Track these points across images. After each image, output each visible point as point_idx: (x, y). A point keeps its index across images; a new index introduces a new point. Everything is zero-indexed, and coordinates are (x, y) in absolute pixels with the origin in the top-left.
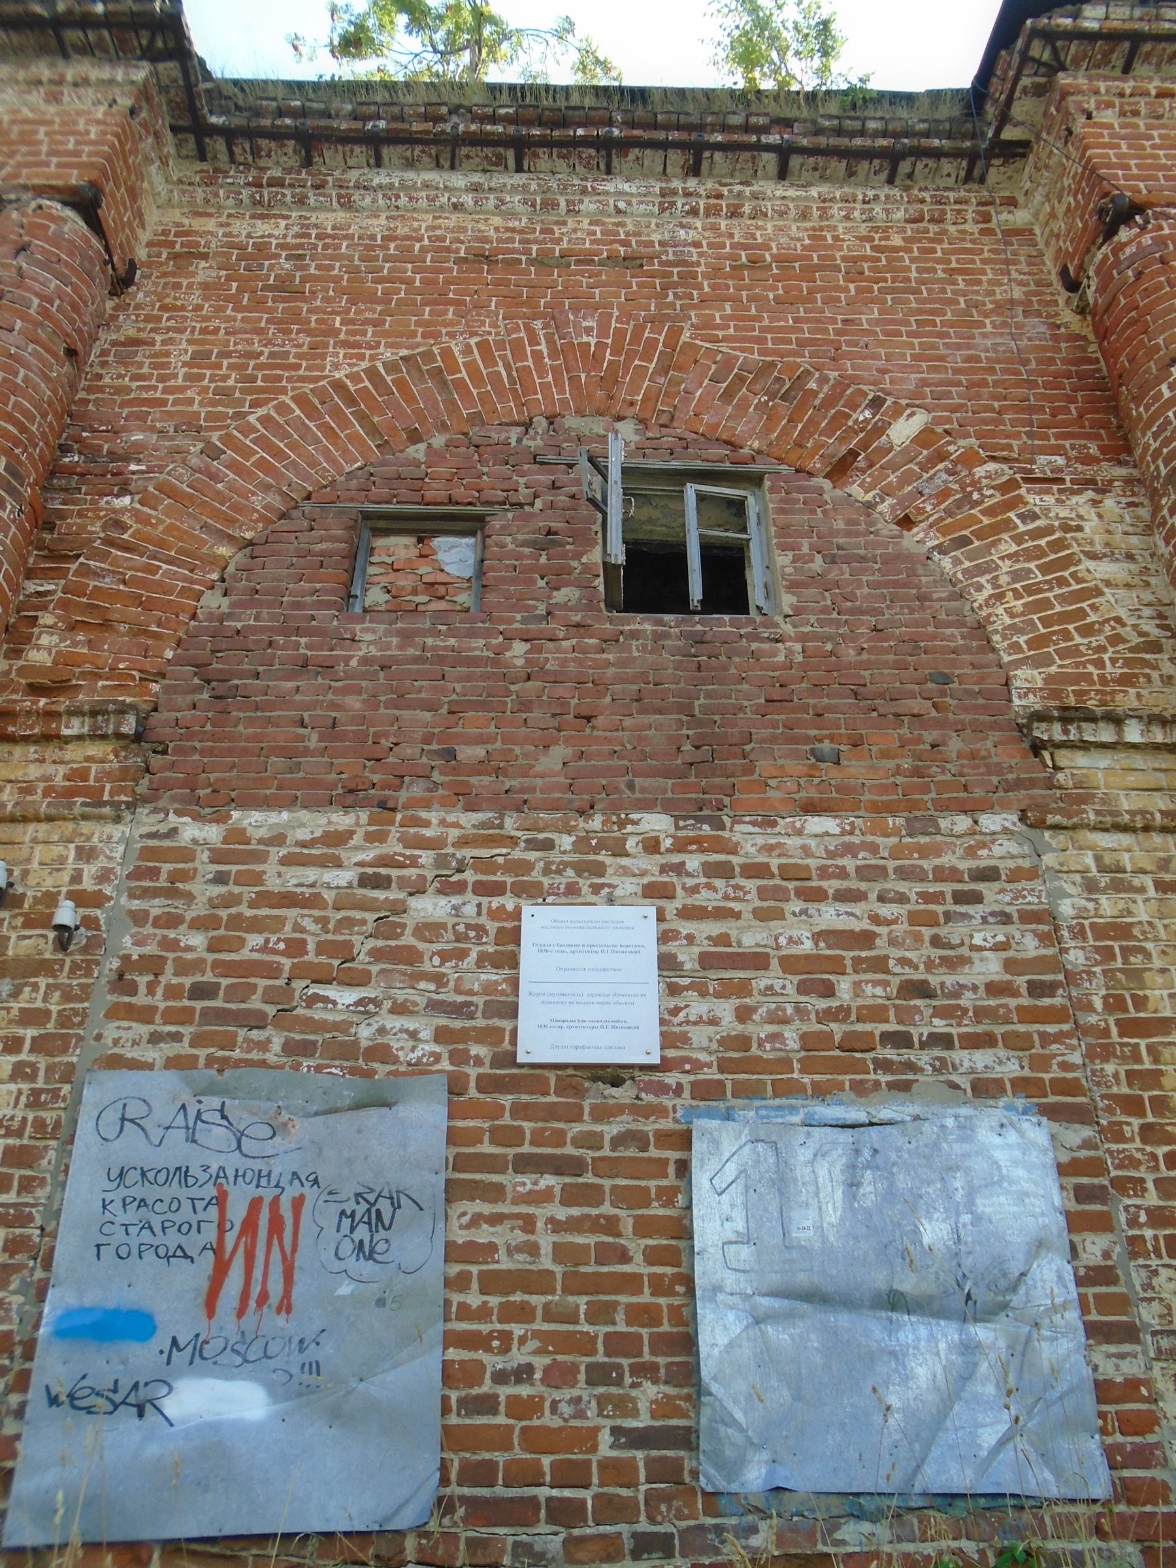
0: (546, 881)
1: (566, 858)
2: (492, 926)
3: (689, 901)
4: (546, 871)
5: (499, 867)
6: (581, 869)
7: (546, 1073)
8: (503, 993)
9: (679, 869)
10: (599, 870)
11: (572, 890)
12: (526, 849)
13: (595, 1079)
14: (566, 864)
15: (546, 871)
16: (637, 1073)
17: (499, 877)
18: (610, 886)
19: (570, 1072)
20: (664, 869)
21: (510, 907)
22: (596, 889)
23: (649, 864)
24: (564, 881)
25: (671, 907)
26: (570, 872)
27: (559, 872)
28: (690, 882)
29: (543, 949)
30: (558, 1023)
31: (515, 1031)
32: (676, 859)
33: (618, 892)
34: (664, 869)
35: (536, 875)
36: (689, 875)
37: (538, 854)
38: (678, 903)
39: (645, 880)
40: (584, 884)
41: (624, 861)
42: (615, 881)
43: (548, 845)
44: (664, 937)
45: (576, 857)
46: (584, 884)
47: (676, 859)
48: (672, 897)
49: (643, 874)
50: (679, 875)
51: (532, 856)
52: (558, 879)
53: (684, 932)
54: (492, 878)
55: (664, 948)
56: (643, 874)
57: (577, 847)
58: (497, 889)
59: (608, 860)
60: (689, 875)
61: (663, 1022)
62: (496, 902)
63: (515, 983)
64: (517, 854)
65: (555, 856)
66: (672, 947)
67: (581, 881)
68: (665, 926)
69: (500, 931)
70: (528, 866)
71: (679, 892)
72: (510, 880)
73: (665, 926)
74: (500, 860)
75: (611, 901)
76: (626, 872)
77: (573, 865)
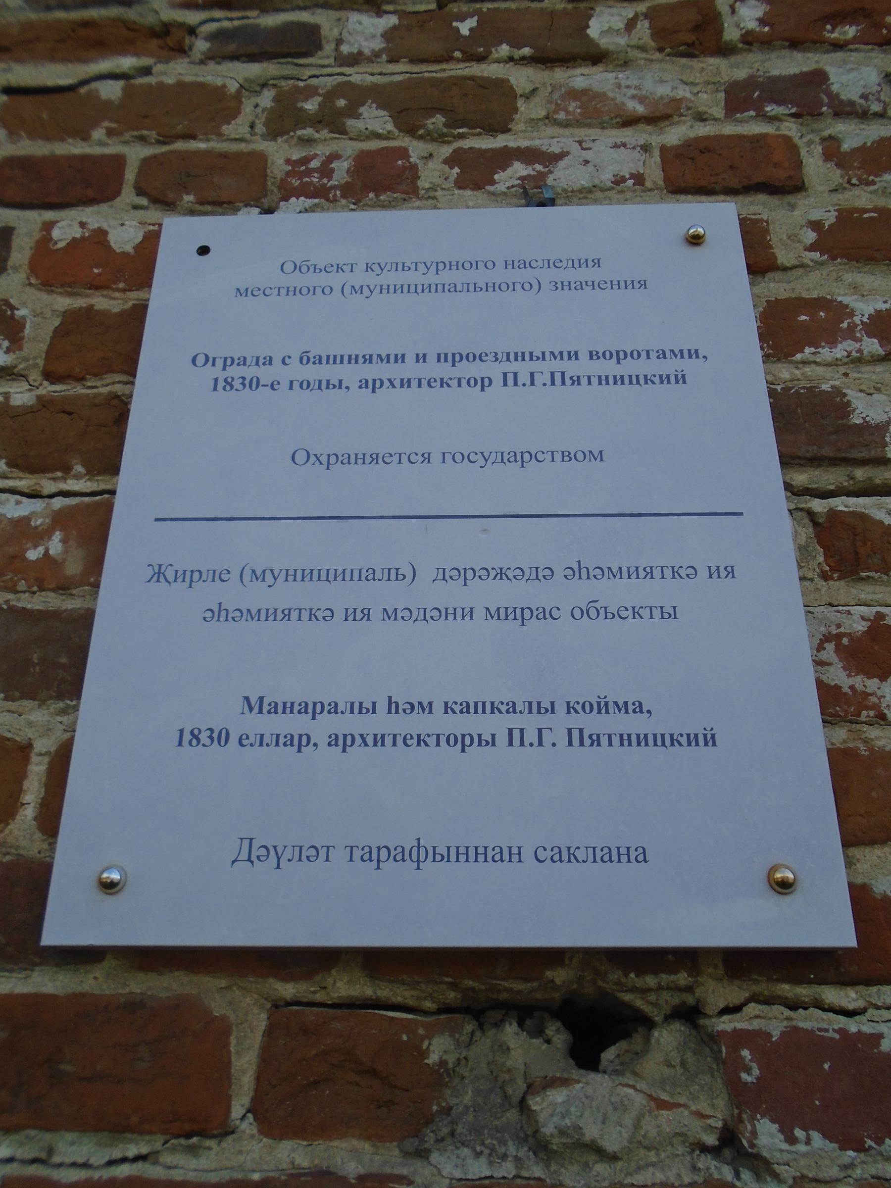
0: (279, 155)
1: (358, 76)
2: (41, 311)
3: (861, 198)
4: (284, 120)
5: (104, 110)
6: (409, 109)
7: (217, 995)
8: (47, 576)
9: (808, 96)
10: (491, 108)
11: (381, 181)
12: (209, 57)
13: (481, 1012)
14: (358, 97)
15: (284, 120)
16: (716, 993)
17: (99, 143)
18: (529, 155)
19: (344, 986)
20: (739, 98)
21: (124, 236)
22: (476, 173)
23: (693, 85)
24: (349, 148)
25: (792, 224)
26: (374, 118)
27: (332, 121)
28: (853, 135)
29: (234, 375)
30: (288, 722)
31: (61, 760)
32: (788, 64)
33: (564, 176)
34: (739, 98)
35: (241, 133)
36: (845, 110)
37: (254, 70)
38: (819, 205)
39: (674, 135)
40: (431, 163)
41: (582, 78)
42: (549, 140)
43: (302, 43)
44: (783, 330)
45: (400, 71)
46: (431, 163)
47: (788, 64)
48: (790, 186)
49: (657, 118)
50: (807, 112)
51: (231, 75)
52: (326, 145)
53: (864, 308)
54: (74, 148)
55: (785, 372)
56: (657, 118)
57: (395, 47)
58: (94, 183)
59: (521, 78)
60: (845, 110)
61: (834, 704)
62: (67, 227)
63: (92, 527)
64: (175, 72)
65: (319, 73)
66: (820, 367)
67: (416, 149)
68: (777, 288)
69: (73, 325)
70: (219, 106)
71: (814, 165)
72: (135, 154)
73: (777, 288)
74: (111, 91)
75: (535, 195)
76: (595, 113)
77: (382, 96)
